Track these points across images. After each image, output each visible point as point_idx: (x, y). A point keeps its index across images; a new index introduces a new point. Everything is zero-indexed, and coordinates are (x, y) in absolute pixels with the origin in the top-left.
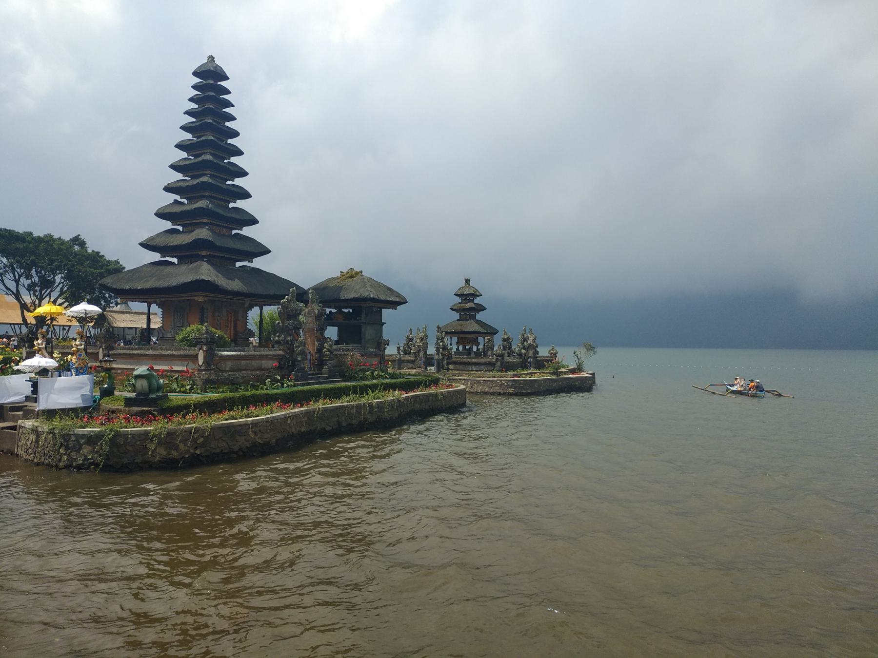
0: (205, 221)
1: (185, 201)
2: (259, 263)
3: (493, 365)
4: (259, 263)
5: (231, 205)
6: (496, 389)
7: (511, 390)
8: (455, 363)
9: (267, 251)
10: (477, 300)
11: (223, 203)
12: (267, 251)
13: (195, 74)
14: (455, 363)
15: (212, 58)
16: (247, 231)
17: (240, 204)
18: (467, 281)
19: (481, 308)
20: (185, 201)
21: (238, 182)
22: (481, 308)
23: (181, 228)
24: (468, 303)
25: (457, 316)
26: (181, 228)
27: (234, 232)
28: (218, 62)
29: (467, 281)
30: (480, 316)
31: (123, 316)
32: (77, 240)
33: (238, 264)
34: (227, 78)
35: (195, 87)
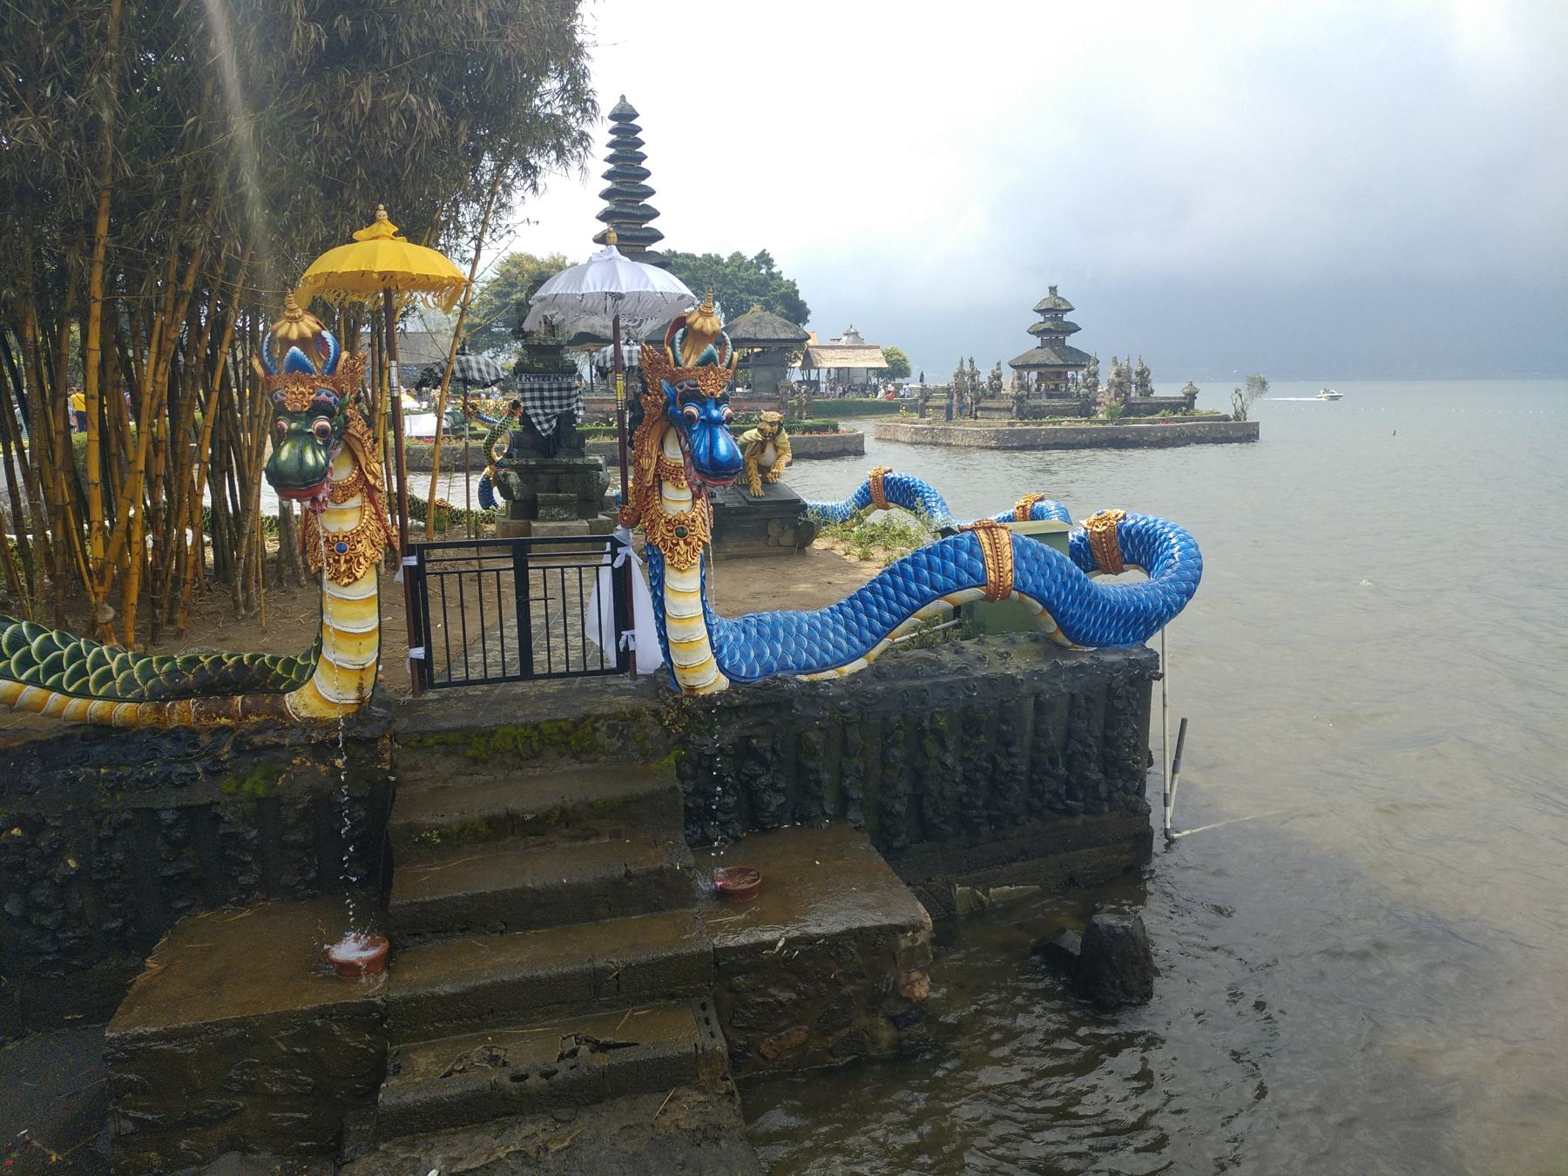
3: (1009, 410)
6: (980, 442)
7: (993, 443)
8: (983, 409)
10: (1067, 318)
11: (638, 249)
14: (983, 409)
15: (623, 97)
18: (1053, 290)
19: (1073, 329)
21: (652, 224)
22: (1073, 329)
24: (1054, 322)
25: (1037, 341)
28: (629, 101)
29: (1053, 290)
30: (1071, 341)
31: (832, 353)
32: (764, 259)
35: (612, 132)
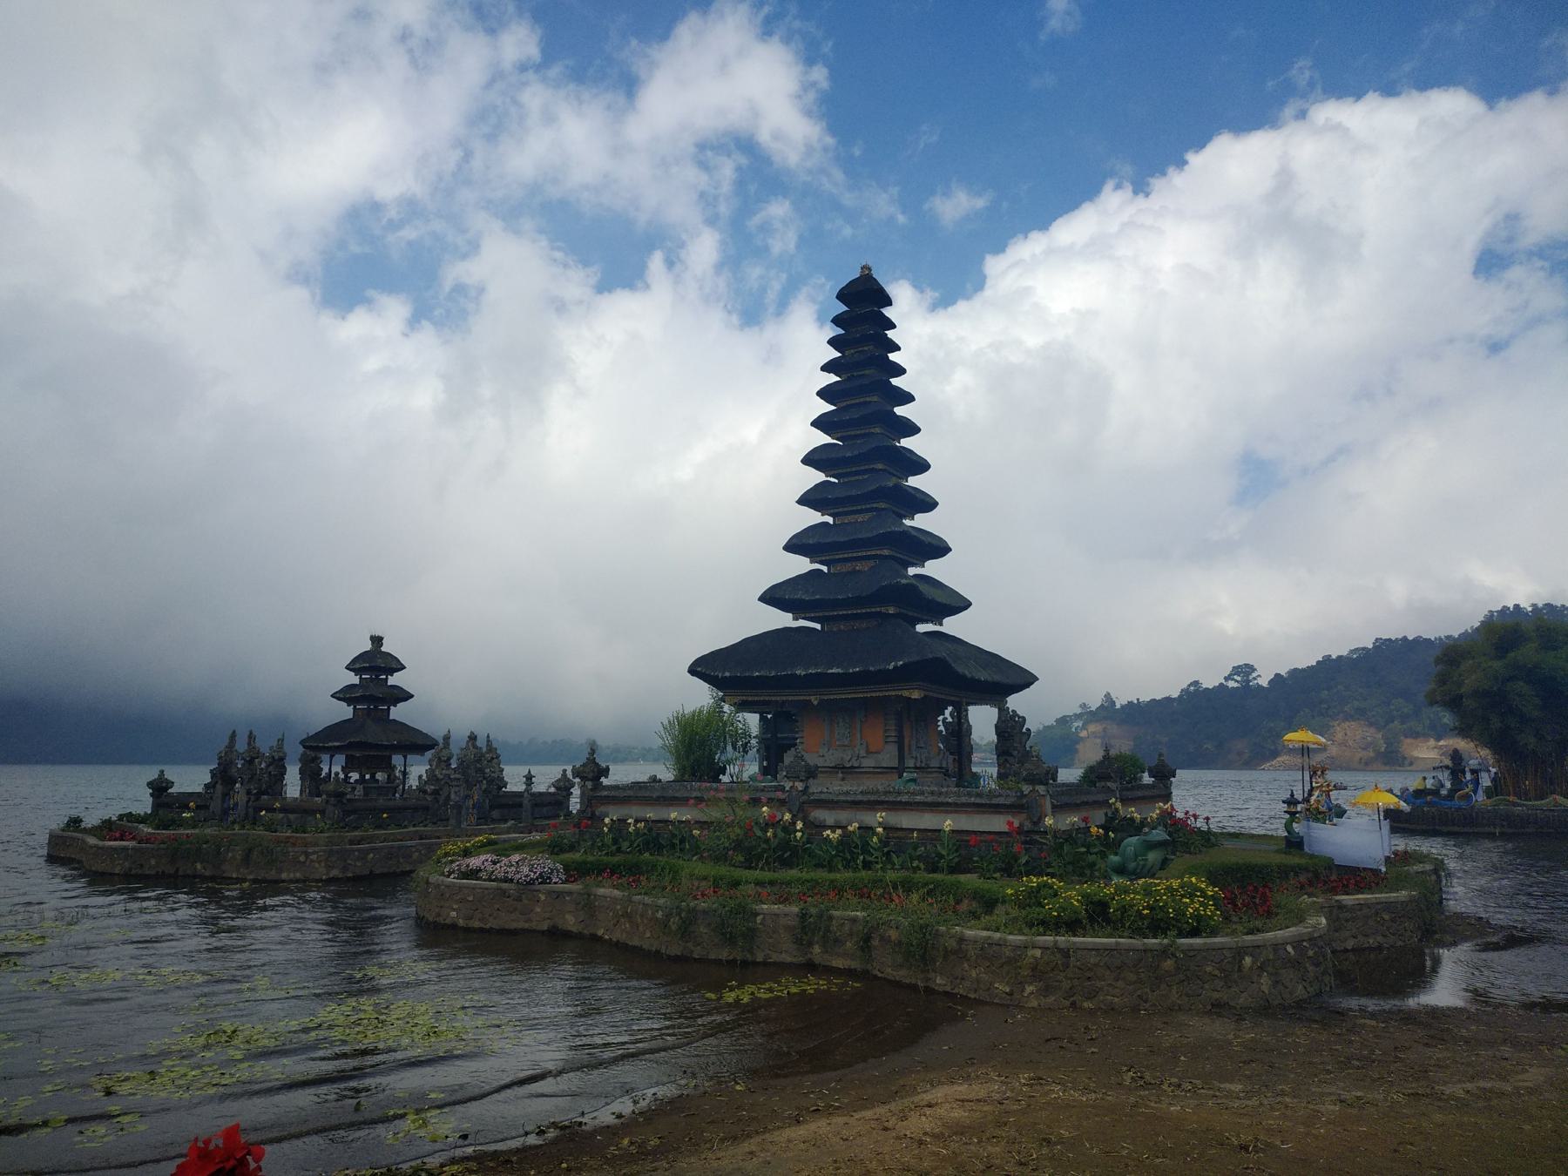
0: (886, 552)
1: (830, 520)
2: (952, 625)
4: (952, 625)
5: (907, 522)
9: (965, 605)
12: (965, 605)
13: (842, 296)
16: (932, 568)
17: (921, 521)
20: (830, 520)
23: (825, 569)
26: (825, 569)
27: (912, 571)
33: (922, 628)
34: (888, 302)
